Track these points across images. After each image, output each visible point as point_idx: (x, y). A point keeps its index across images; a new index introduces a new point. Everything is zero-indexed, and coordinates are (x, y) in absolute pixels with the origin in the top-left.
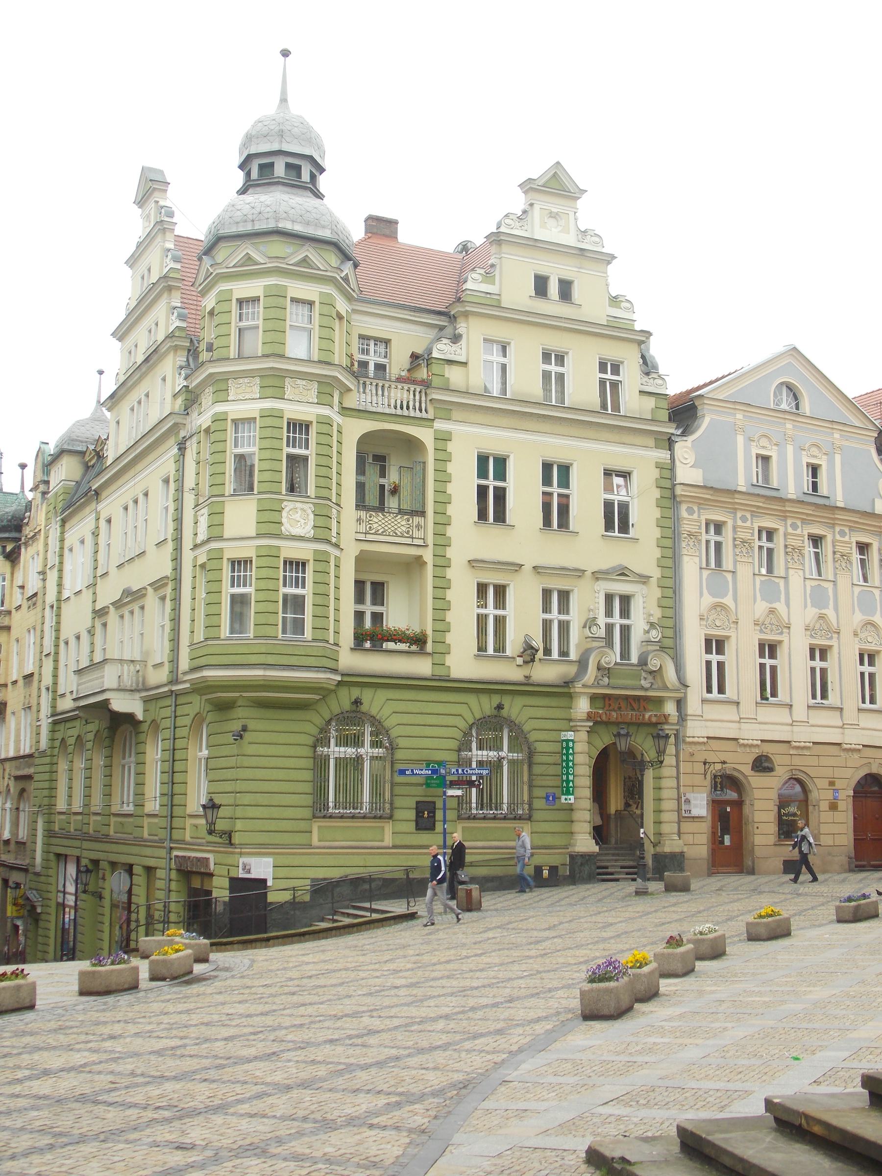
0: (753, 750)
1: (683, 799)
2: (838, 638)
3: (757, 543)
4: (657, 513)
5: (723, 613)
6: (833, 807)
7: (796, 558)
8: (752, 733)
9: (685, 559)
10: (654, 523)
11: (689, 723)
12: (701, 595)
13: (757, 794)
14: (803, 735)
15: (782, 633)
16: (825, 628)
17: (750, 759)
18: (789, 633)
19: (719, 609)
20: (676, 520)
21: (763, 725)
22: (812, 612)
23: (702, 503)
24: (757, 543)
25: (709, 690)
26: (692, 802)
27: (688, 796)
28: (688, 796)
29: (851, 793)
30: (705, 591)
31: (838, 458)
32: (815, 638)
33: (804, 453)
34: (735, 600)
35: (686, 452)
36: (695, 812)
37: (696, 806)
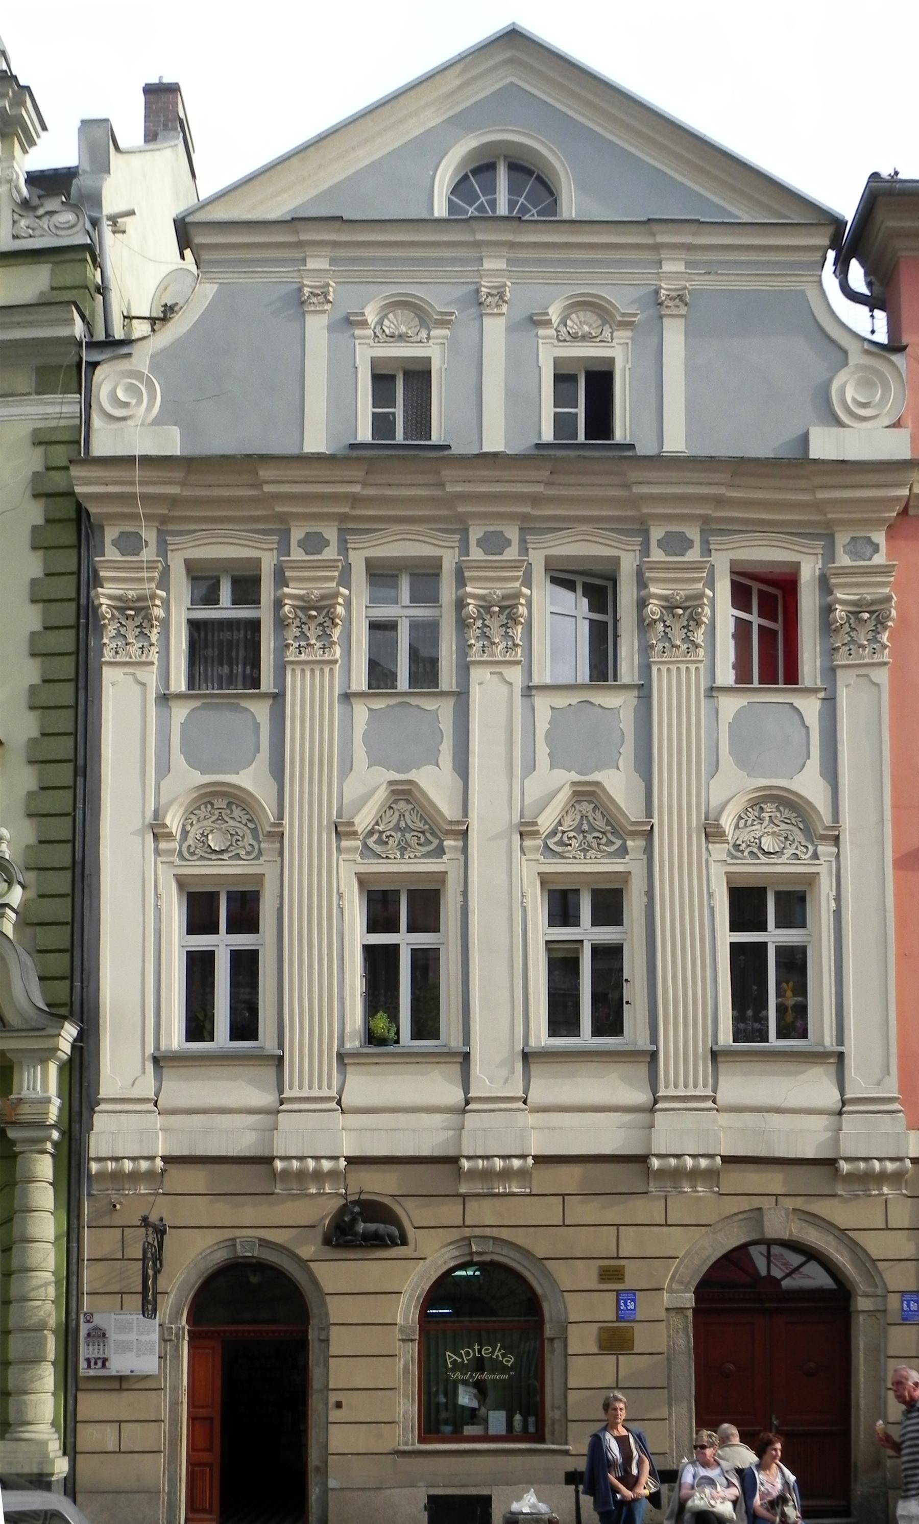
1: (84, 1329)
4: (32, 566)
5: (237, 812)
6: (615, 1341)
10: (24, 591)
12: (164, 769)
13: (337, 1310)
15: (440, 851)
16: (600, 823)
18: (465, 850)
19: (221, 803)
21: (363, 1114)
23: (170, 518)
26: (114, 1336)
27: (98, 1320)
28: (98, 1320)
29: (688, 1299)
30: (177, 758)
34: (278, 770)
36: (119, 1364)
37: (124, 1347)
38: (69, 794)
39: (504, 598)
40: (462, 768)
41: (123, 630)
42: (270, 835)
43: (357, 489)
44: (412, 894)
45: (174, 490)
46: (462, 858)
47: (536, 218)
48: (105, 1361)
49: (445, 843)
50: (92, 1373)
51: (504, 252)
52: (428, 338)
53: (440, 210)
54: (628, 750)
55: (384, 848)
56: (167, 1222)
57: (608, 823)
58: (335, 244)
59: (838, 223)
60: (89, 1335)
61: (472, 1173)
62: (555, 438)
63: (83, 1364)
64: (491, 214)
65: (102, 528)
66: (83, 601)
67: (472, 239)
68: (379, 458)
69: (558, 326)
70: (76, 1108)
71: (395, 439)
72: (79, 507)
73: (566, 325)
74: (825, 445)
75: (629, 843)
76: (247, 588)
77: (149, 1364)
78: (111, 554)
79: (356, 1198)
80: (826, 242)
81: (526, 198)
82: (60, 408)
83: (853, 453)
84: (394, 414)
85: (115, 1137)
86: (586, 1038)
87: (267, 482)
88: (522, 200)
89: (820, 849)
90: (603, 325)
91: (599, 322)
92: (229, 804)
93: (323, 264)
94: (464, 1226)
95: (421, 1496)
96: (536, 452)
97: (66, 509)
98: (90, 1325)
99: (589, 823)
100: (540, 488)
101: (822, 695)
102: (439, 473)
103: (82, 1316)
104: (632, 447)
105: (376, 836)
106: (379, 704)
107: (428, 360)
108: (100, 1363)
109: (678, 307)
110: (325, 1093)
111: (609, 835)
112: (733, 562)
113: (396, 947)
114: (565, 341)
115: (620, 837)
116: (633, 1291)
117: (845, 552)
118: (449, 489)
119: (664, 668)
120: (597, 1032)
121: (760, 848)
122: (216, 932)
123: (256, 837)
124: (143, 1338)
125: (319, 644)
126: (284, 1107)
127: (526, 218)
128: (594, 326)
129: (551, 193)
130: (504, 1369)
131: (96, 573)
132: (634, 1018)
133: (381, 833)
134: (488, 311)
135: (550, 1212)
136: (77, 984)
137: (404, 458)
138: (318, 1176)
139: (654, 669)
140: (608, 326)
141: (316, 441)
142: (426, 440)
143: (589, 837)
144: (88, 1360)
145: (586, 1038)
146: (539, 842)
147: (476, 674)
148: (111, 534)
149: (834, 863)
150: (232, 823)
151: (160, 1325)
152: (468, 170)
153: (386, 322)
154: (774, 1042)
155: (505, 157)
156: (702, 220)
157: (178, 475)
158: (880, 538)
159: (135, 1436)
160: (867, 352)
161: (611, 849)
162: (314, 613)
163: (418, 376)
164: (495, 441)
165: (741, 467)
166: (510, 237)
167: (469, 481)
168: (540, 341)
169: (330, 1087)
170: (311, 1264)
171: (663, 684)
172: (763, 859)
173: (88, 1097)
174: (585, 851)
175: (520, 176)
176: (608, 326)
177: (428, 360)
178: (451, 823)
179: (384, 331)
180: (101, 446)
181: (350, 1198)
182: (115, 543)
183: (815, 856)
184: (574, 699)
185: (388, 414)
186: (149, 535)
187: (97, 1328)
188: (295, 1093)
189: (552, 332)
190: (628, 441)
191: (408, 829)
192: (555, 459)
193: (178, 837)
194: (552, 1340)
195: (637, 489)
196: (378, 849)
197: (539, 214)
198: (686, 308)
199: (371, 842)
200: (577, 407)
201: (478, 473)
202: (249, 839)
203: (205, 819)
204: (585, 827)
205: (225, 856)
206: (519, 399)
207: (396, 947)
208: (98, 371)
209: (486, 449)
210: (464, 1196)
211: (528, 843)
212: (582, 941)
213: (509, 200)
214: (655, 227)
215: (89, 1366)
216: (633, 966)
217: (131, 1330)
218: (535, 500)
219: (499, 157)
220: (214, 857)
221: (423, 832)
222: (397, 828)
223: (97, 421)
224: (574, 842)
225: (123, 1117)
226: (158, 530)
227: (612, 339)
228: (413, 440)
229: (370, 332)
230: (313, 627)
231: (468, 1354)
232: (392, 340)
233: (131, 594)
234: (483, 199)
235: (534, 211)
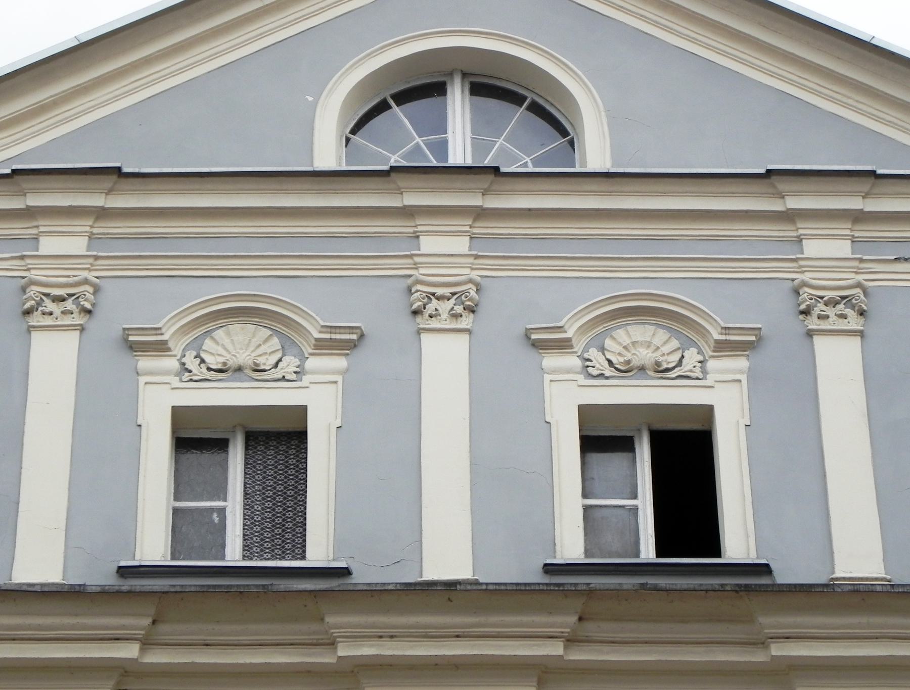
31: (839, 364)
43: (130, 651)
47: (531, 169)
52: (299, 373)
58: (102, 214)
62: (587, 553)
64: (434, 163)
67: (398, 204)
68: (180, 594)
69: (586, 349)
71: (223, 558)
73: (602, 349)
81: (420, 137)
84: (222, 511)
91: (675, 343)
93: (77, 245)
96: (546, 579)
100: (556, 649)
102: (322, 620)
104: (764, 569)
107: (301, 412)
109: (843, 316)
114: (601, 376)
118: (343, 651)
128: (666, 349)
129: (564, 132)
134: (434, 324)
137: (241, 593)
140: (693, 350)
142: (294, 558)
152: (387, 95)
153: (208, 344)
155: (464, 75)
156: (879, 172)
163: (279, 440)
164: (448, 556)
166: (475, 200)
167: (392, 637)
168: (547, 378)
176: (693, 350)
177: (301, 412)
179: (203, 361)
185: (211, 510)
189: (574, 362)
190: (752, 557)
192: (590, 593)
195: (777, 650)
197: (536, 163)
198: (861, 320)
200: (635, 497)
201: (413, 619)
206: (500, 477)
209: (431, 573)
214: (782, 185)
219: (451, 74)
227: (704, 372)
228: (261, 558)
229: (172, 363)
232: (221, 376)
234: (418, 140)
235: (528, 159)
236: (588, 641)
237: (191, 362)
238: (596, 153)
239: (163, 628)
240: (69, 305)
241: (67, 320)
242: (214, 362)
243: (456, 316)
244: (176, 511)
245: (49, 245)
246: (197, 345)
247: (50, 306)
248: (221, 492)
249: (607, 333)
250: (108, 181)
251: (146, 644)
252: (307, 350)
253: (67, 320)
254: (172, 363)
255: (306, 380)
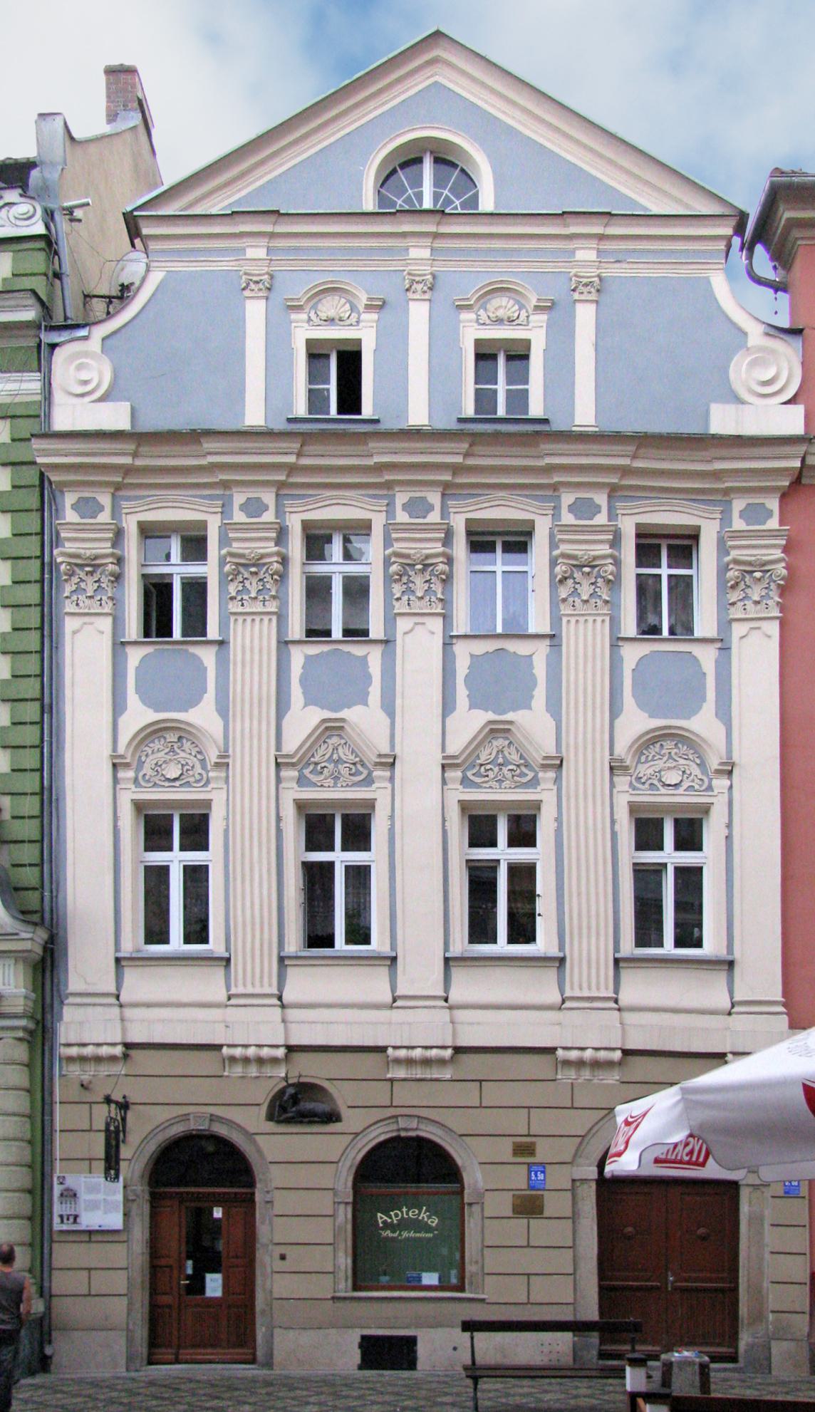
0: (268, 1071)
1: (57, 1189)
2: (557, 780)
3: (209, 570)
5: (187, 745)
7: (420, 590)
8: (260, 1030)
9: (70, 624)
11: (69, 1014)
14: (422, 1030)
15: (368, 781)
16: (514, 757)
17: (263, 1093)
18: (392, 779)
19: (172, 737)
20: (46, 536)
22: (468, 723)
24: (209, 570)
25: (157, 933)
26: (84, 1196)
28: (71, 1181)
31: (585, 316)
32: (477, 786)
33: (465, 316)
34: (223, 709)
35: (80, 367)
36: (90, 1220)
37: (94, 1206)
38: (36, 728)
39: (427, 557)
40: (389, 707)
41: (83, 585)
42: (217, 765)
44: (346, 818)
45: (127, 460)
46: (389, 786)
47: (459, 211)
48: (76, 1217)
49: (375, 773)
50: (65, 1227)
51: (428, 242)
53: (369, 203)
54: (540, 694)
55: (322, 777)
56: (132, 1099)
57: (521, 757)
58: (272, 235)
59: (742, 217)
60: (62, 1195)
61: (398, 1061)
62: (476, 412)
63: (56, 1220)
65: (62, 492)
66: (47, 559)
70: (48, 1000)
71: (328, 413)
72: (42, 474)
74: (723, 421)
75: (541, 775)
76: (195, 546)
77: (115, 1220)
78: (71, 516)
79: (295, 1080)
80: (729, 232)
82: (26, 386)
83: (751, 427)
84: (328, 390)
85: (83, 1027)
86: (502, 946)
87: (210, 453)
88: (446, 192)
89: (714, 782)
90: (520, 309)
92: (180, 738)
94: (391, 1106)
95: (354, 1337)
97: (31, 476)
98: (62, 1187)
99: (504, 757)
100: (459, 459)
101: (719, 645)
103: (55, 1179)
105: (311, 767)
106: (313, 650)
107: (359, 342)
108: (72, 1219)
110: (267, 990)
111: (523, 769)
112: (638, 525)
113: (331, 865)
115: (532, 769)
116: (543, 1164)
117: (741, 517)
119: (573, 620)
120: (512, 940)
121: (660, 780)
122: (170, 849)
123: (204, 767)
124: (109, 1198)
125: (261, 598)
126: (233, 1001)
127: (447, 211)
130: (428, 1228)
131: (58, 534)
132: (544, 928)
133: (316, 764)
135: (470, 1095)
136: (47, 894)
138: (260, 1061)
139: (565, 620)
141: (254, 416)
143: (505, 770)
144: (61, 1217)
145: (502, 946)
146: (459, 774)
147: (403, 625)
148: (70, 499)
149: (726, 795)
150: (182, 755)
151: (125, 1187)
153: (320, 306)
154: (668, 947)
157: (131, 447)
158: (773, 504)
159: (101, 1282)
160: (767, 334)
161: (524, 780)
162: (253, 569)
164: (418, 416)
165: (645, 441)
166: (433, 229)
169: (270, 985)
170: (257, 1137)
171: (571, 633)
172: (663, 791)
173: (58, 991)
174: (500, 781)
175: (443, 167)
177: (359, 342)
178: (380, 756)
180: (61, 421)
181: (290, 1081)
182: (74, 507)
183: (710, 788)
184: (490, 646)
186: (105, 499)
187: (67, 1190)
188: (241, 990)
191: (339, 761)
193: (134, 766)
194: (470, 1204)
196: (314, 778)
199: (306, 772)
202: (198, 769)
203: (158, 751)
204: (500, 760)
205: (177, 784)
207: (331, 865)
208: (57, 350)
210: (392, 1080)
211: (449, 774)
212: (498, 861)
213: (435, 193)
214: (569, 220)
215: (62, 1222)
216: (544, 884)
217: (98, 1191)
218: (456, 469)
220: (167, 784)
221: (354, 764)
222: (330, 760)
223: (58, 396)
224: (490, 773)
225: (90, 1009)
226: (113, 495)
229: (304, 317)
230: (254, 581)
231: (396, 1215)
233: (88, 553)
235: (457, 203)
236: (473, 455)
237: (313, 315)
238: (487, 203)
239: (305, 448)
240: (261, 286)
241: (261, 294)
242: (324, 316)
243: (425, 292)
244: (310, 391)
245: (251, 253)
246: (314, 307)
247: (252, 286)
248: (327, 381)
249: (486, 303)
250: (273, 218)
251: (299, 455)
252: (361, 309)
253: (261, 294)
254: (304, 317)
255: (361, 324)
